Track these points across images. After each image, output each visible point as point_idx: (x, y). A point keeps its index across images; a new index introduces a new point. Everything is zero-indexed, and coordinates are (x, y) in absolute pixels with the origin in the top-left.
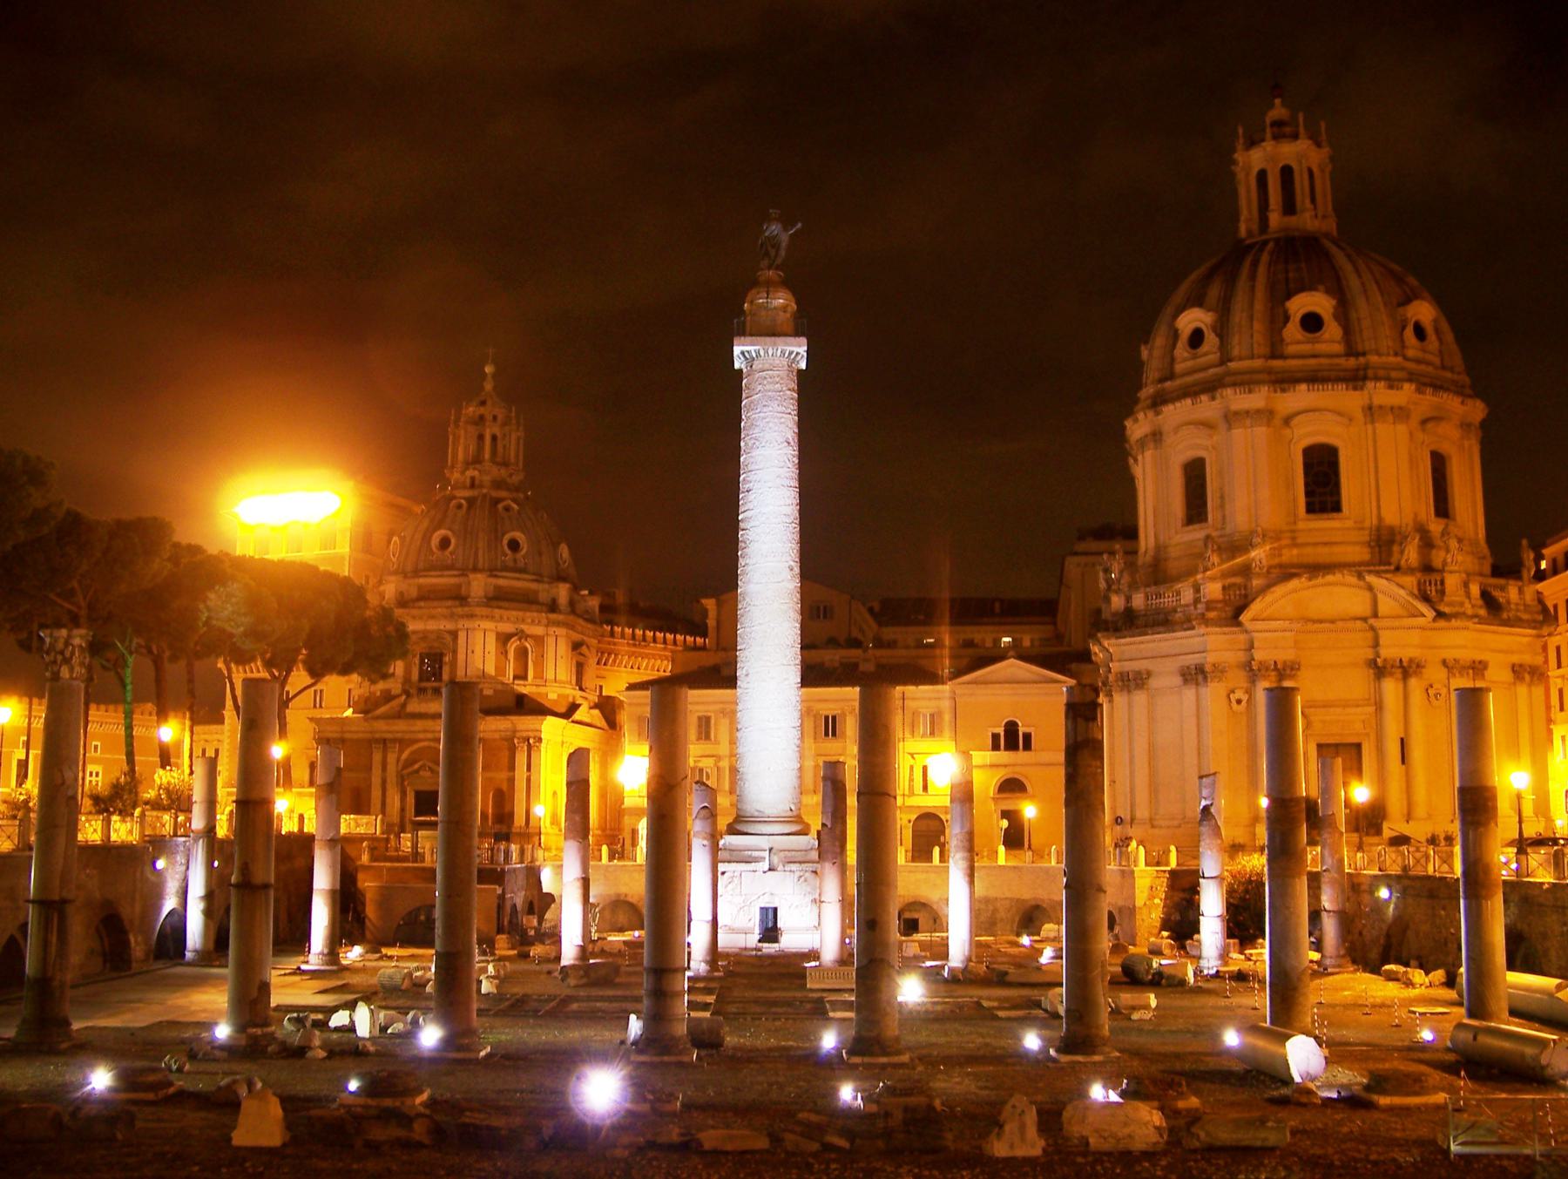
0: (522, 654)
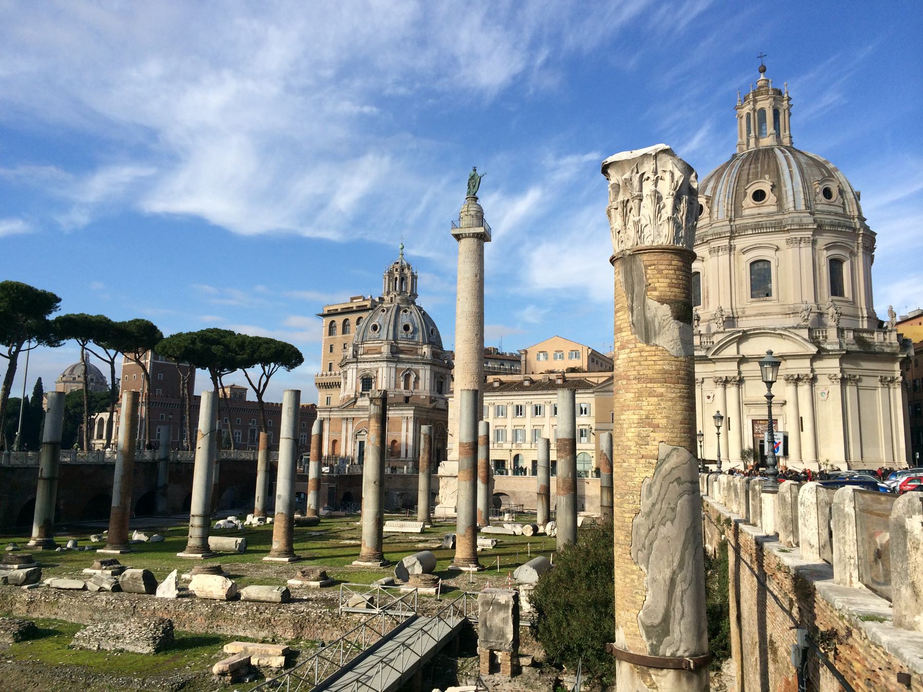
0: (407, 377)
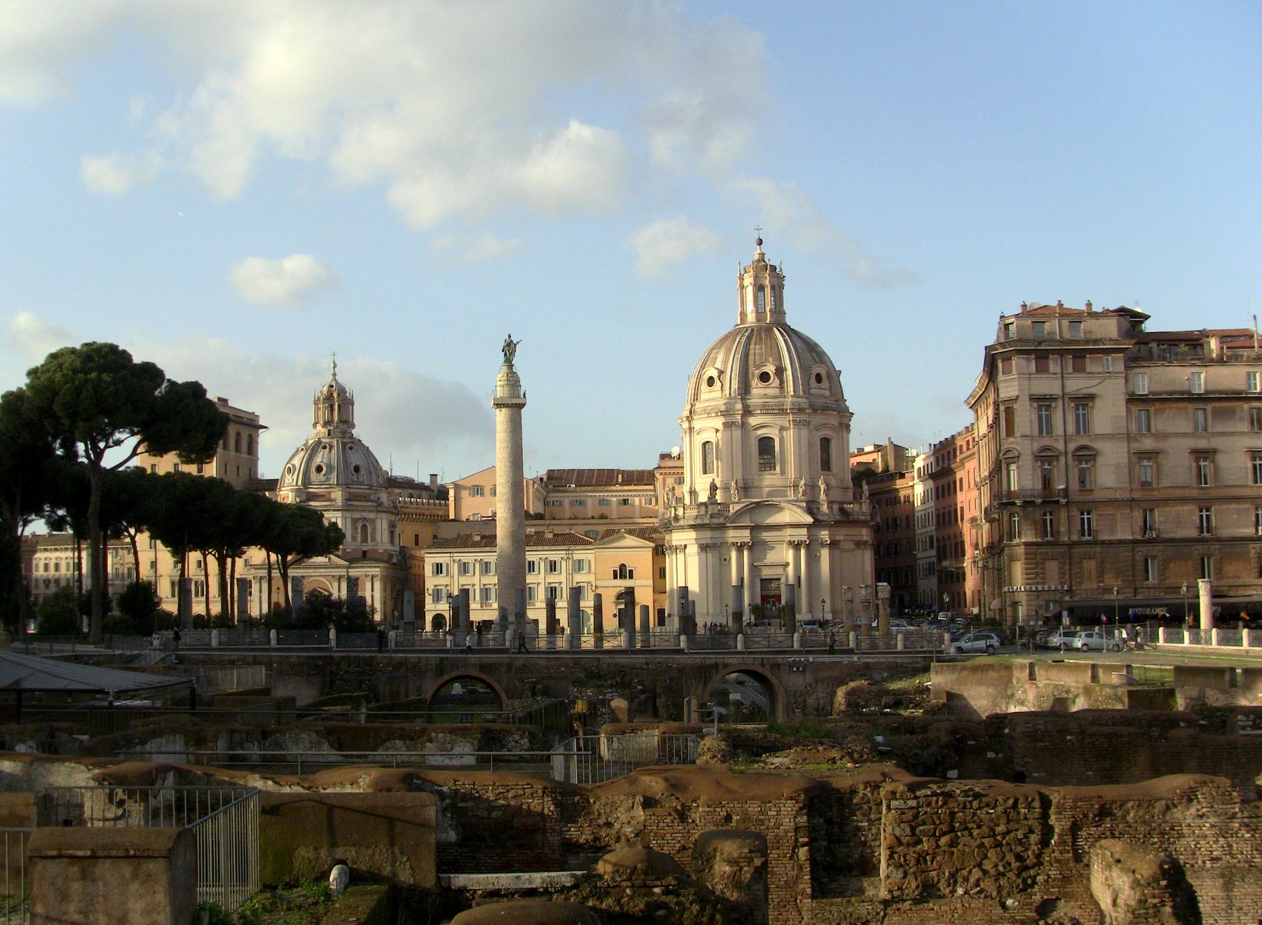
0: (364, 527)
